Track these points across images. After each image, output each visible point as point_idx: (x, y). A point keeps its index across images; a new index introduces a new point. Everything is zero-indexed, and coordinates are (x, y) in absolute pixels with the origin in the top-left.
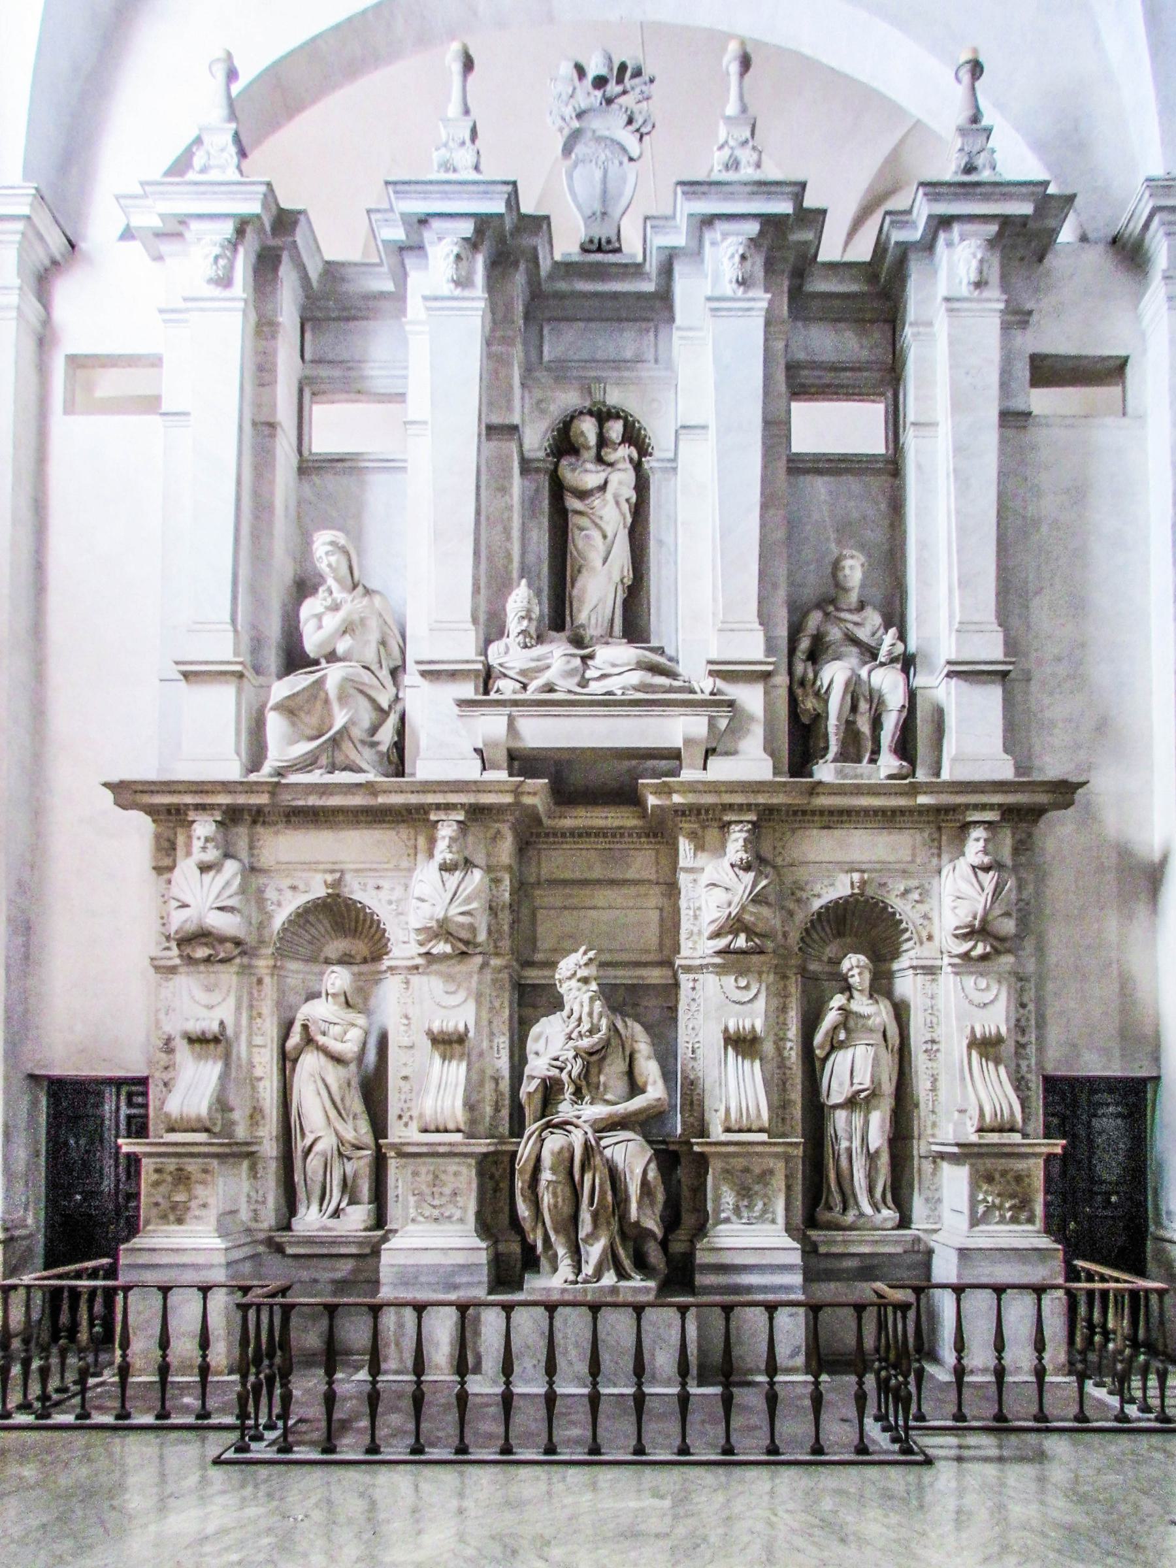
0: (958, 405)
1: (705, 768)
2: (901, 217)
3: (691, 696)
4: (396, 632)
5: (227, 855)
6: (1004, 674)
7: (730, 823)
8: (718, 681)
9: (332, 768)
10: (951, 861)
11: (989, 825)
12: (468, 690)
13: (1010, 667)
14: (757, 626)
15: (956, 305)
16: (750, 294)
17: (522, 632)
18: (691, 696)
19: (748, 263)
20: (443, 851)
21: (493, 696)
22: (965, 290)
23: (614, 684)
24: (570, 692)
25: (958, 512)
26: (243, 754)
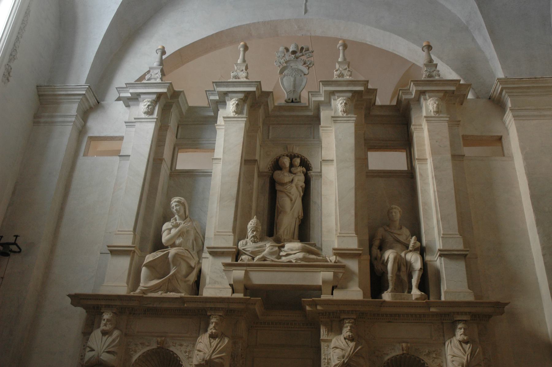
0: (434, 152)
1: (332, 294)
2: (408, 92)
3: (326, 263)
4: (201, 236)
5: (116, 328)
6: (465, 256)
7: (344, 319)
8: (338, 258)
9: (167, 291)
10: (449, 338)
11: (465, 322)
12: (229, 260)
13: (467, 253)
14: (354, 235)
15: (431, 119)
16: (349, 115)
17: (253, 236)
18: (326, 263)
19: (348, 106)
20: (211, 329)
21: (239, 262)
22: (432, 114)
23: (292, 258)
24: (272, 261)
25: (438, 191)
26: (130, 286)
